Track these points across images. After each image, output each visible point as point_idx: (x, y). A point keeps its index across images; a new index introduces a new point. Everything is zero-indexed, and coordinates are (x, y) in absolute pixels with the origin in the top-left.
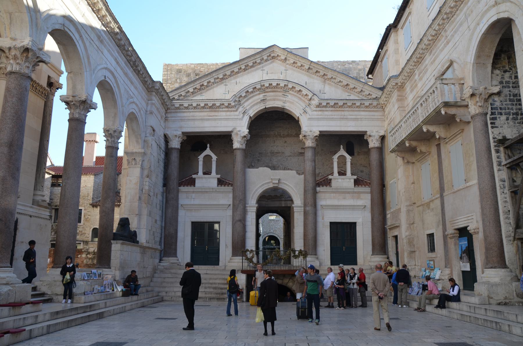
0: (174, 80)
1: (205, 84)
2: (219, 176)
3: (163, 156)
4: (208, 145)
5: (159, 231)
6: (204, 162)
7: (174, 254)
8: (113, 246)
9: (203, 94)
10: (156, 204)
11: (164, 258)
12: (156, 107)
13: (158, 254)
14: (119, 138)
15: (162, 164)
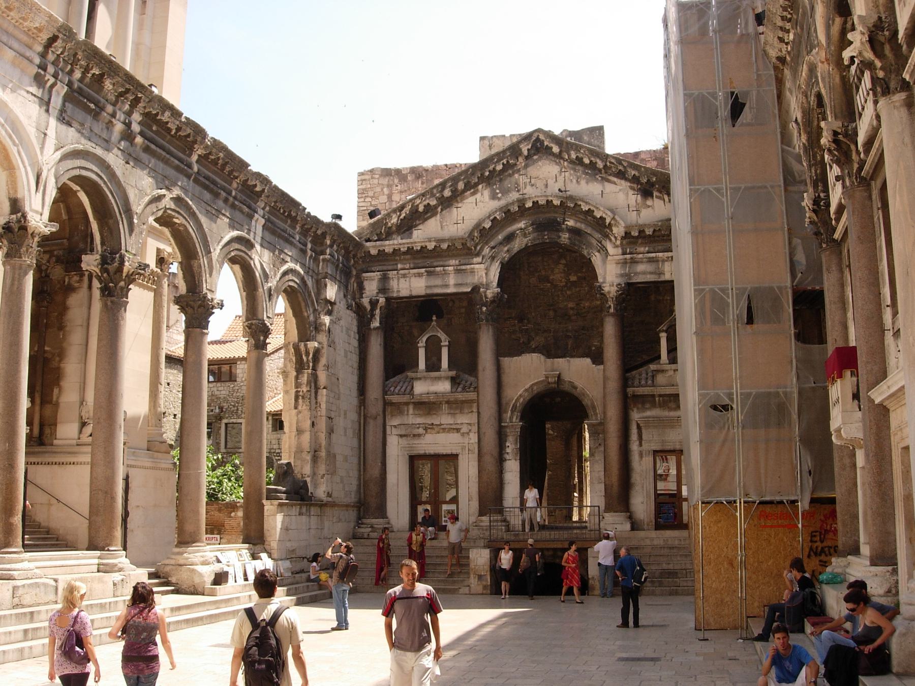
0: (378, 189)
1: (421, 209)
2: (453, 373)
3: (356, 343)
4: (434, 318)
5: (354, 474)
6: (426, 348)
7: (381, 511)
8: (266, 508)
9: (420, 227)
10: (345, 429)
11: (364, 521)
12: (333, 263)
13: (352, 514)
14: (266, 337)
15: (355, 358)
